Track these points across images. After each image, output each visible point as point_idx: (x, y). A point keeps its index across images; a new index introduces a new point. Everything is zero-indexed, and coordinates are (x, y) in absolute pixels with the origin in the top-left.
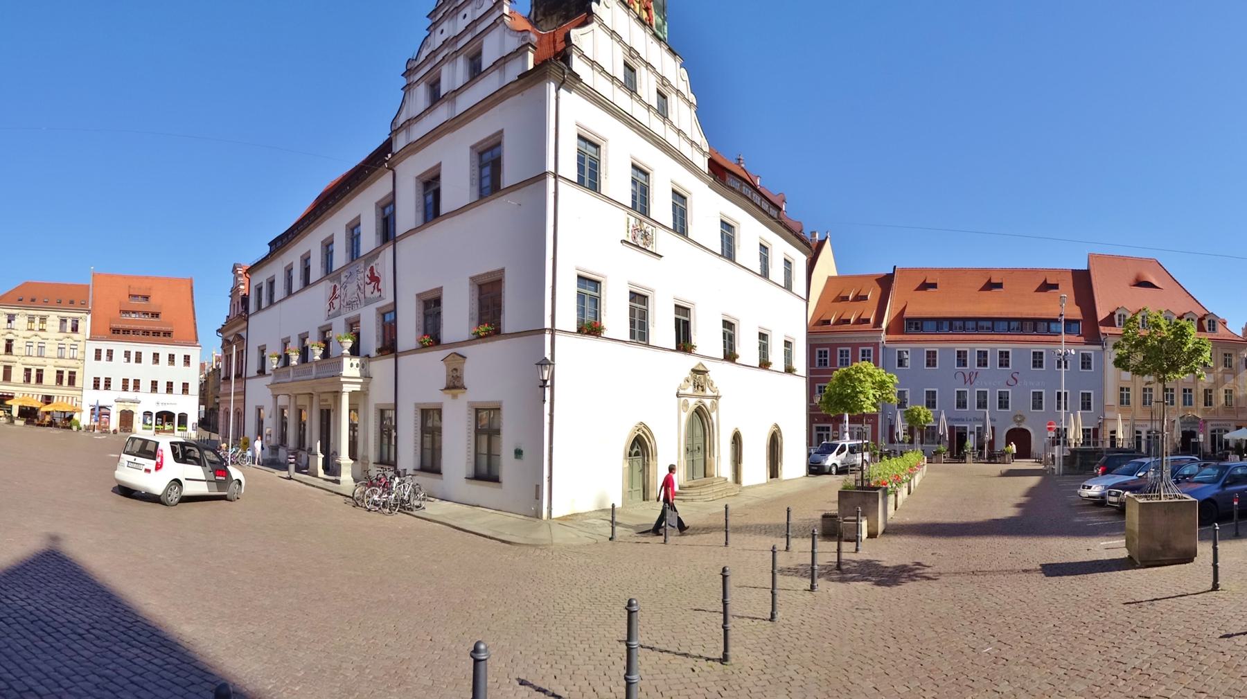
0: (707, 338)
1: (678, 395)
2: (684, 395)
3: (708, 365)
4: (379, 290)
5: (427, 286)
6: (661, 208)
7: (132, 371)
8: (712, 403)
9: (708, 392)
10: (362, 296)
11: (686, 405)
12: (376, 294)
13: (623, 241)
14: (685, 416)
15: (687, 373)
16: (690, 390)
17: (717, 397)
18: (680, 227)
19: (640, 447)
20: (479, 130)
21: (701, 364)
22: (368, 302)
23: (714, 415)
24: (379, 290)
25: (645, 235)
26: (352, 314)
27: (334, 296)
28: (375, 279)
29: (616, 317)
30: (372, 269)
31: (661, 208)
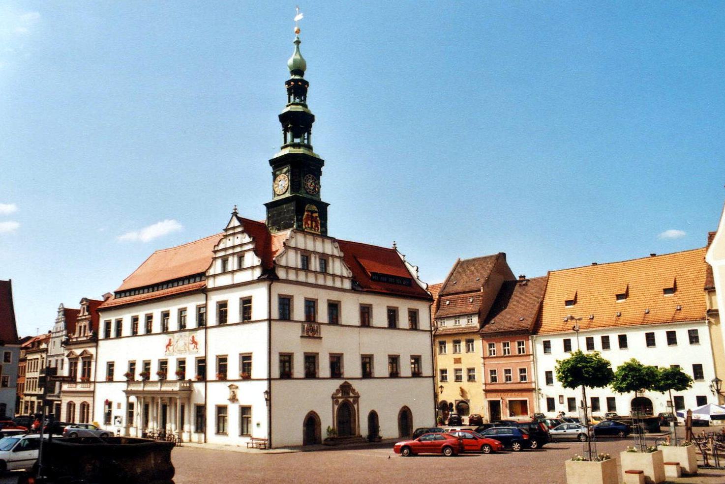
0: (352, 368)
1: (333, 398)
2: (336, 398)
3: (350, 382)
4: (197, 348)
5: (221, 353)
6: (323, 315)
8: (354, 401)
9: (351, 394)
10: (187, 349)
11: (337, 402)
12: (195, 350)
13: (302, 337)
14: (336, 407)
15: (338, 387)
16: (340, 395)
18: (334, 318)
19: (312, 421)
20: (245, 293)
21: (346, 382)
22: (190, 353)
23: (356, 406)
24: (197, 348)
25: (313, 330)
26: (181, 356)
27: (169, 344)
28: (194, 342)
29: (299, 368)
30: (193, 337)
31: (323, 315)
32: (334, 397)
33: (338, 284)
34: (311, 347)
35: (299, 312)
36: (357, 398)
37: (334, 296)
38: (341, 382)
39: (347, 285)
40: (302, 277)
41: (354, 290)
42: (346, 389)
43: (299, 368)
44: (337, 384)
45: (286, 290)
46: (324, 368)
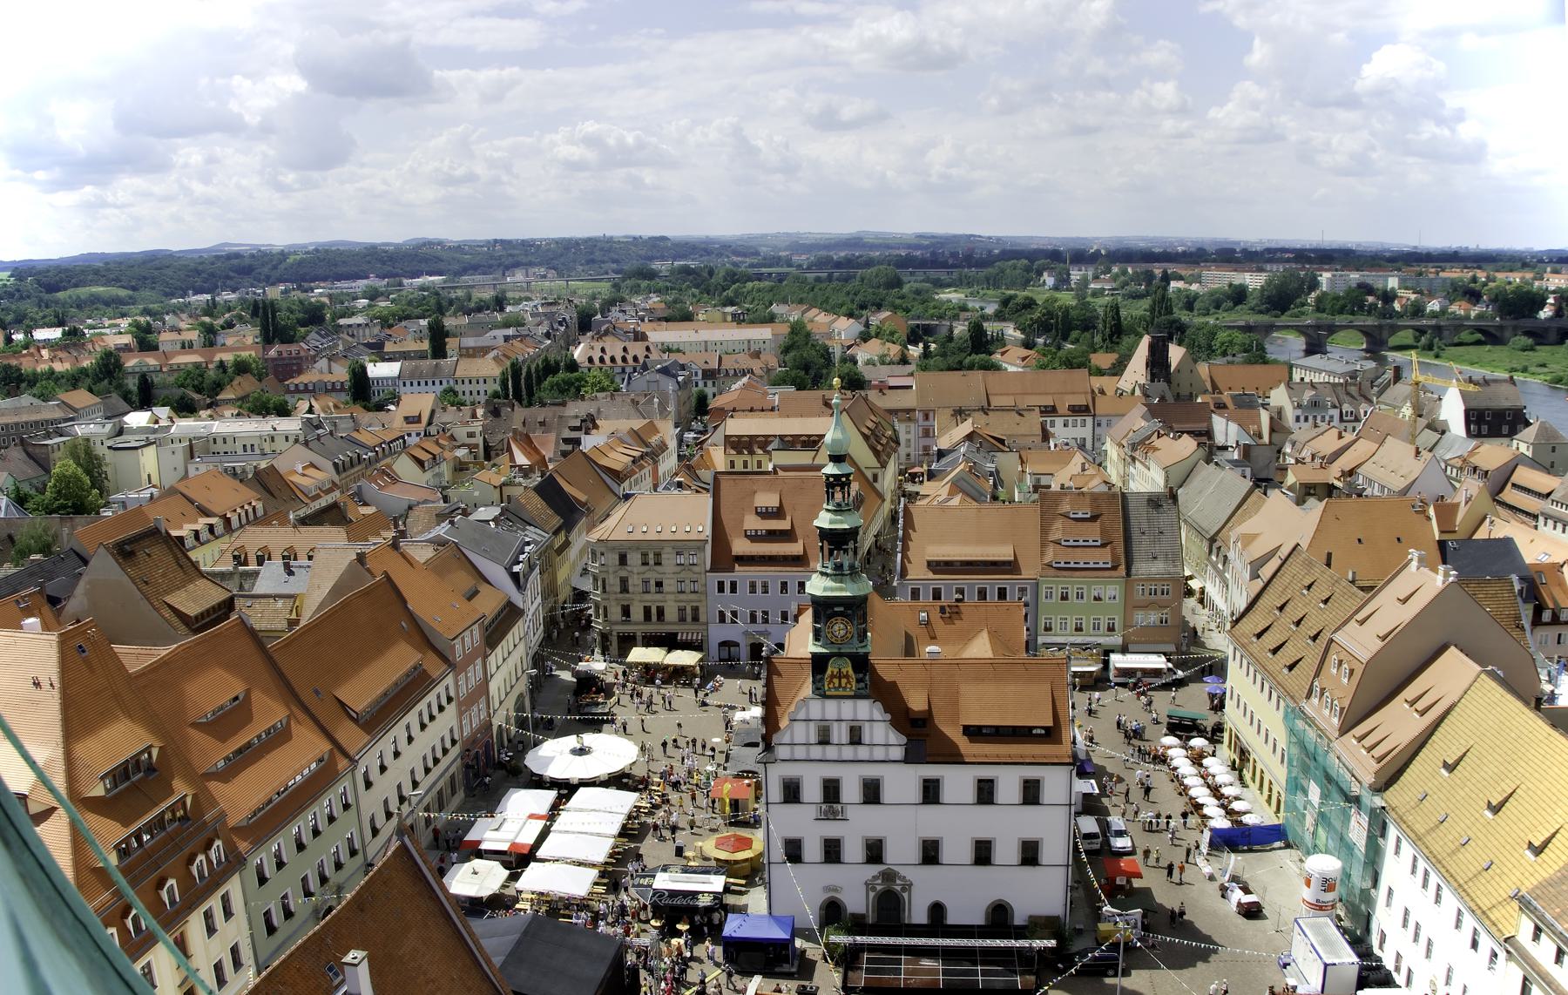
7: (760, 602)
11: (874, 889)
14: (872, 894)
17: (911, 885)
23: (906, 895)
29: (813, 851)
31: (851, 792)
32: (869, 886)
33: (879, 753)
34: (832, 830)
35: (812, 791)
36: (908, 887)
37: (872, 771)
38: (881, 868)
39: (897, 753)
40: (817, 752)
41: (911, 758)
42: (889, 876)
43: (813, 851)
44: (875, 869)
45: (791, 771)
46: (853, 851)
